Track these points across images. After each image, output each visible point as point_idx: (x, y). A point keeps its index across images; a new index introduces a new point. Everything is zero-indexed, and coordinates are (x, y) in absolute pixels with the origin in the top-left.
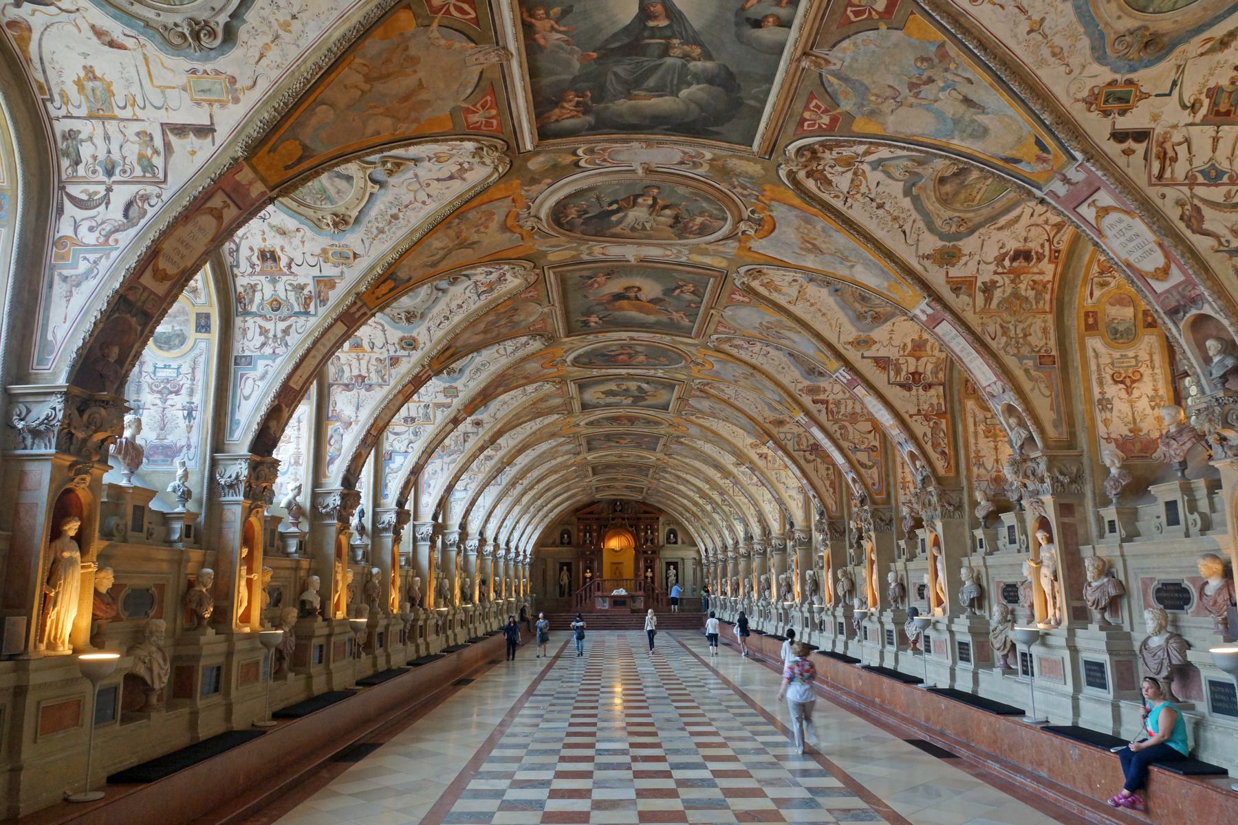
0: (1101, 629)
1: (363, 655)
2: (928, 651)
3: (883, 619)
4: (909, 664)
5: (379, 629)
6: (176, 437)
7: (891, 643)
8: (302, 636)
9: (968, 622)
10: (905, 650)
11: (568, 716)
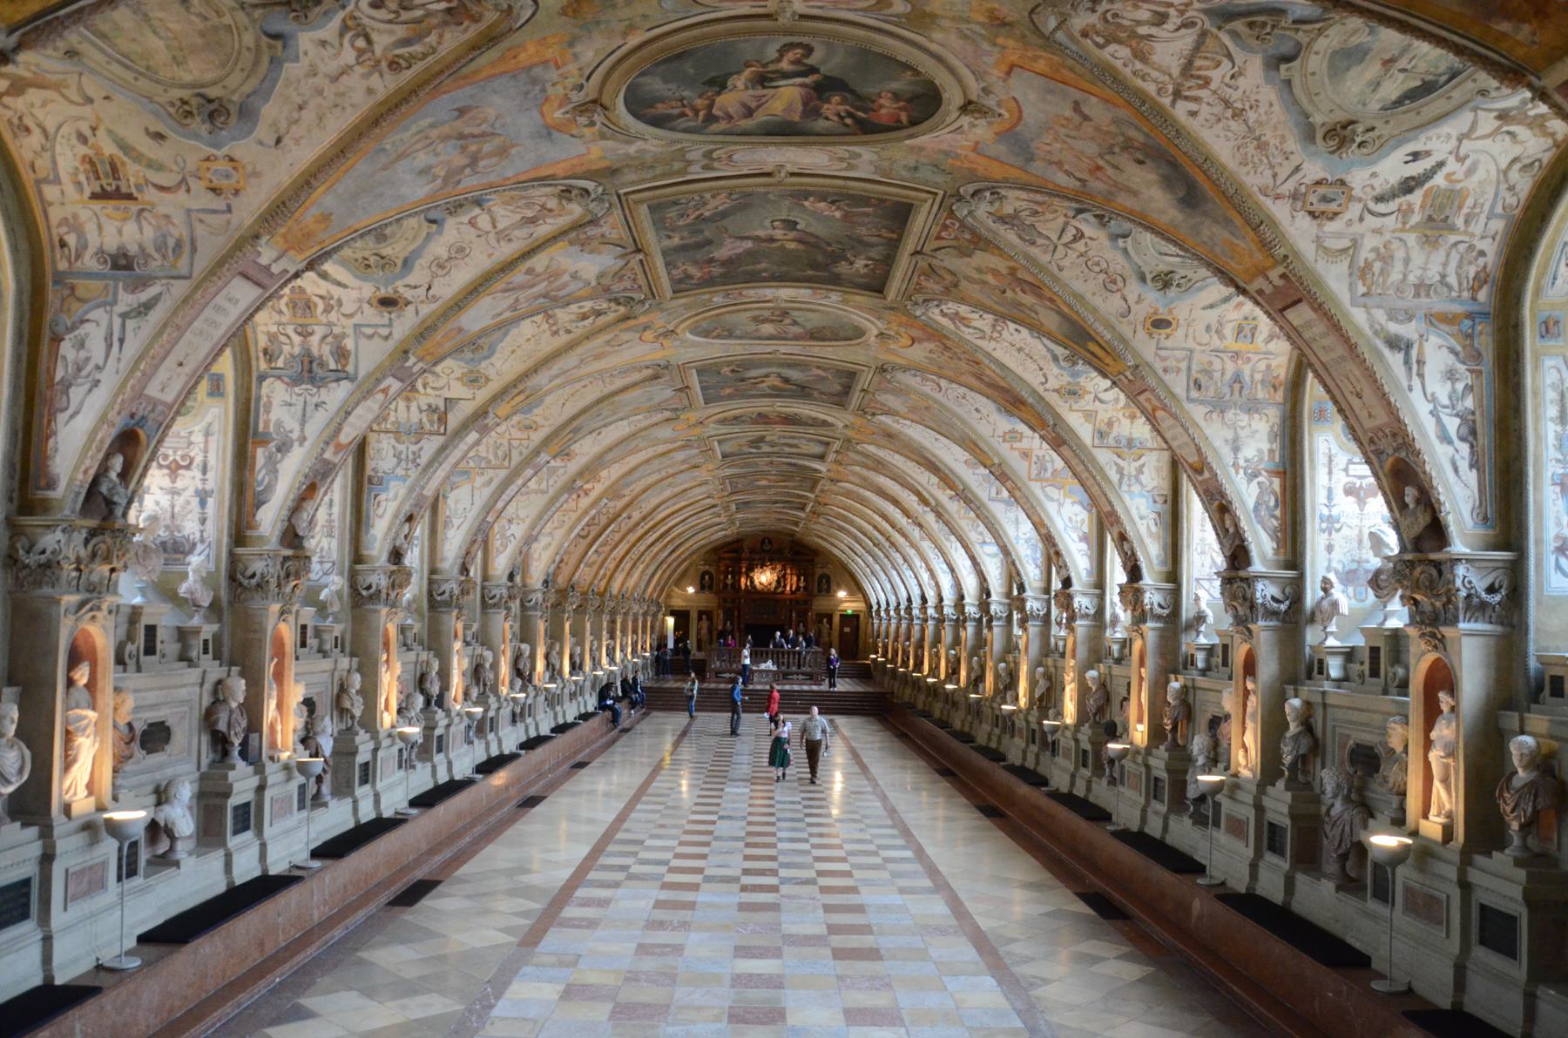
0: (1287, 788)
1: (419, 765)
2: (1122, 783)
3: (1080, 736)
4: (1102, 793)
5: (438, 732)
6: (190, 528)
7: (1085, 765)
8: (345, 749)
9: (1166, 755)
10: (1100, 776)
11: (675, 843)
